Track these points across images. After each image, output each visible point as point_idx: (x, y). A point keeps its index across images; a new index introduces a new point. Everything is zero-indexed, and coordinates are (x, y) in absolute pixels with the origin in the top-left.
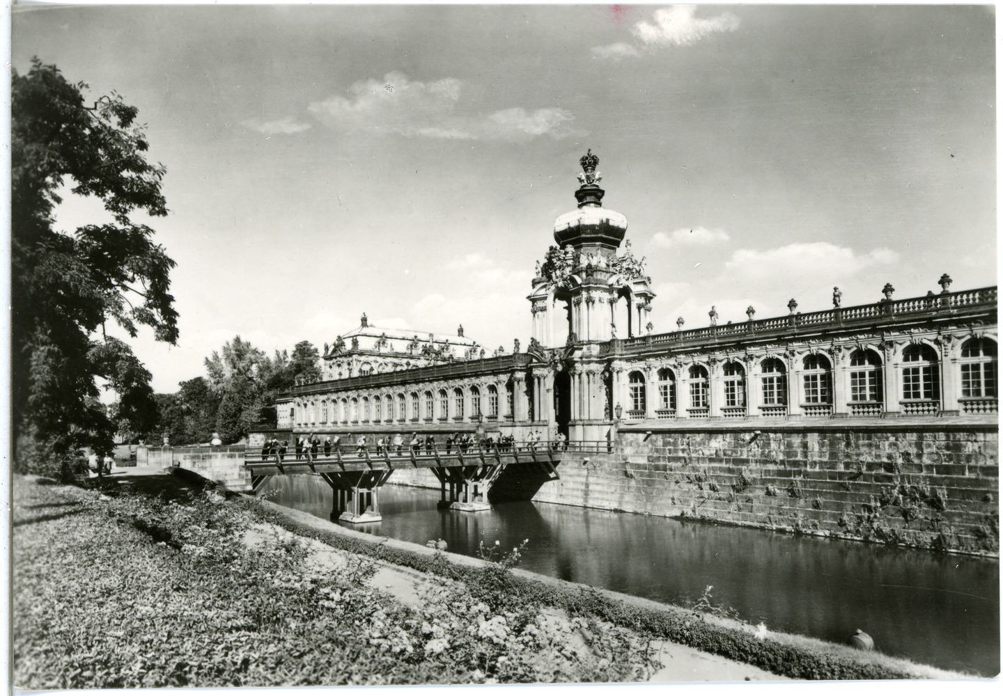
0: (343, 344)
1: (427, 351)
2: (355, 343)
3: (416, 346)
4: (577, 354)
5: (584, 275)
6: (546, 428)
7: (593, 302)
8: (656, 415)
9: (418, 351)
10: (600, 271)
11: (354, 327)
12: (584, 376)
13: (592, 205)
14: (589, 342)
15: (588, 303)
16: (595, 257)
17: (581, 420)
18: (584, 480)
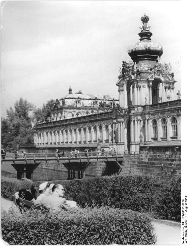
0: (59, 103)
1: (102, 105)
2: (64, 103)
3: (96, 103)
4: (133, 111)
5: (135, 75)
6: (124, 146)
7: (140, 88)
8: (161, 140)
9: (97, 105)
10: (143, 73)
11: (66, 94)
12: (136, 121)
13: (145, 40)
14: (138, 106)
15: (137, 88)
16: (144, 66)
17: (134, 142)
18: (129, 169)
